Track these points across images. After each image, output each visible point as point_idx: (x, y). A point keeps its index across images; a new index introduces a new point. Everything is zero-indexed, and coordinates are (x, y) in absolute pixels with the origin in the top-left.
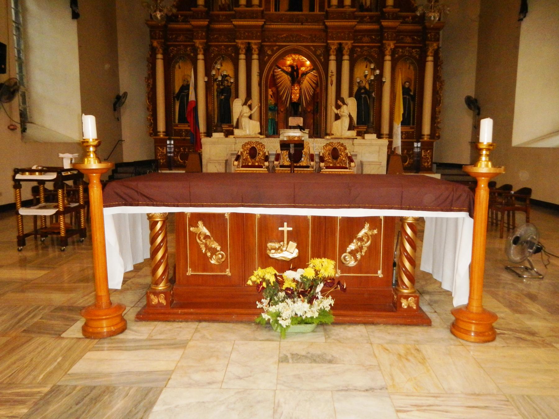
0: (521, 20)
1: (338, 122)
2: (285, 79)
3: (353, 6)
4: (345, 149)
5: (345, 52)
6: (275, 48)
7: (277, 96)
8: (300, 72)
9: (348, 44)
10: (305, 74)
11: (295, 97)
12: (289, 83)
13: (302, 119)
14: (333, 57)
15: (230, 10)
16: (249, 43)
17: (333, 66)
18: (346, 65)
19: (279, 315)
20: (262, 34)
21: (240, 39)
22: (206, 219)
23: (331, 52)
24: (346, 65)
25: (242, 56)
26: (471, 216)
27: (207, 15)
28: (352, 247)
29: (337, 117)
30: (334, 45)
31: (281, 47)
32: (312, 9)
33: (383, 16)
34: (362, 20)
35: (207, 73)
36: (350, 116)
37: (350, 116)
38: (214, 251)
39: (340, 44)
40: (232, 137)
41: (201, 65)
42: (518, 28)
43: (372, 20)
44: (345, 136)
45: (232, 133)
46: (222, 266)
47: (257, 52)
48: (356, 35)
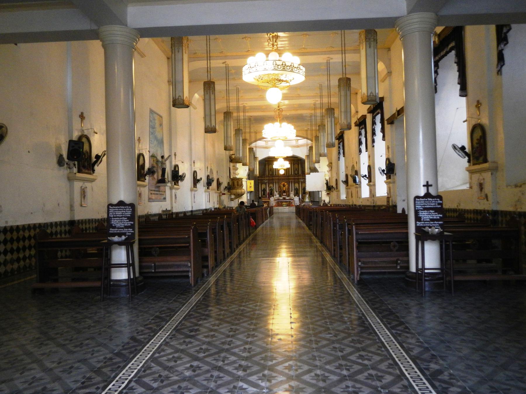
2: (282, 186)
9: (293, 181)
20: (278, 179)
27: (269, 177)
33: (299, 176)
35: (268, 186)
41: (267, 185)
48: (294, 179)
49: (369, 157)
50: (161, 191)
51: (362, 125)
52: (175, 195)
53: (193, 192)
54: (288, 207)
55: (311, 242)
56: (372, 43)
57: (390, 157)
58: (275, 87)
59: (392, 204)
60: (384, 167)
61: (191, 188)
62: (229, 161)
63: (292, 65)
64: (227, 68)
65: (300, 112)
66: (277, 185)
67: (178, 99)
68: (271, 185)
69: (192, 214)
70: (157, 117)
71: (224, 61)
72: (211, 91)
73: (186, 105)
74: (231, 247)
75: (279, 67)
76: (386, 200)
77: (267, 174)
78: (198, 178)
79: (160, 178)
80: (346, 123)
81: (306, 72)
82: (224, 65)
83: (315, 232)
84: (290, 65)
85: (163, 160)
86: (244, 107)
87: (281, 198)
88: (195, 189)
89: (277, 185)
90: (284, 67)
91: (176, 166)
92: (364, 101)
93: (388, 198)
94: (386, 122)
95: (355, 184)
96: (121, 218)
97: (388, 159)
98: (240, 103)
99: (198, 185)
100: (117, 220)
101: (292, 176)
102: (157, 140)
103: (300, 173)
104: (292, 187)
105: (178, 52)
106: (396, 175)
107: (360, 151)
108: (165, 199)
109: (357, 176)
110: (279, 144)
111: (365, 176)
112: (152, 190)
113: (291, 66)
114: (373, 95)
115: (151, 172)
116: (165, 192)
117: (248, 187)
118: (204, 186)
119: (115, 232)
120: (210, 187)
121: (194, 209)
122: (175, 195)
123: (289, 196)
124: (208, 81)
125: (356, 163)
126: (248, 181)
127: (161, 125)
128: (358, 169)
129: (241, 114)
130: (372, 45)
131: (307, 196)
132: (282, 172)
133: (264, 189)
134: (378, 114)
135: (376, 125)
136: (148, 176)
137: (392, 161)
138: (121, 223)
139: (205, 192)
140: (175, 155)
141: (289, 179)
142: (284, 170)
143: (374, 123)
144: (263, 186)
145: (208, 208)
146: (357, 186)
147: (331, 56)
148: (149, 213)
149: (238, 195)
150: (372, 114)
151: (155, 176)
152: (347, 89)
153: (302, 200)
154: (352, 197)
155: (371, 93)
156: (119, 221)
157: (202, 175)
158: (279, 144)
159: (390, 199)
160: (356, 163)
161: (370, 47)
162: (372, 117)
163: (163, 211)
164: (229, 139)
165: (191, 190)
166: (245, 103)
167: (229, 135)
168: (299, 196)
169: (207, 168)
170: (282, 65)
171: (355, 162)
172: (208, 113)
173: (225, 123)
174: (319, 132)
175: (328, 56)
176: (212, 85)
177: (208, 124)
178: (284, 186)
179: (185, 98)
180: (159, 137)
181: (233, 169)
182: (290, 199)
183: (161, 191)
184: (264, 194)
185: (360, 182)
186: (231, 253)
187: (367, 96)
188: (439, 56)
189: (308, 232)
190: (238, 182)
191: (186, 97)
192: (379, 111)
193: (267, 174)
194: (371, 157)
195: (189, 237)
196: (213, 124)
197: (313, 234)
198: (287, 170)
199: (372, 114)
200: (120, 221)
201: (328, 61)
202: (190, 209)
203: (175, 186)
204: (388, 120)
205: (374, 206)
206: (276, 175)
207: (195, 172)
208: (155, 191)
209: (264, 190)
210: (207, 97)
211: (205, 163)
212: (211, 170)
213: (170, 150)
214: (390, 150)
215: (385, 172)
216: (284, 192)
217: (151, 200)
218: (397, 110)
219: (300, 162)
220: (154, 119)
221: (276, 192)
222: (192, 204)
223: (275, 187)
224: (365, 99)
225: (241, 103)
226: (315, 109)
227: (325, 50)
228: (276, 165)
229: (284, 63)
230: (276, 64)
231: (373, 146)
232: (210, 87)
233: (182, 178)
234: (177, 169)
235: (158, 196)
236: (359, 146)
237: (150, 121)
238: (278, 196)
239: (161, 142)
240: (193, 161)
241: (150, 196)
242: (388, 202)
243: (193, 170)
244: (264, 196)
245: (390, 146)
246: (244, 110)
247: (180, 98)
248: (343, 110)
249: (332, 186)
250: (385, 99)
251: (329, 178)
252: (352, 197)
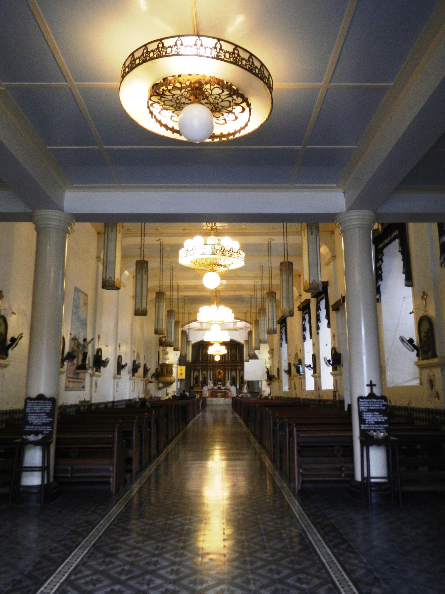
2: (217, 374)
3: (230, 361)
7: (215, 376)
9: (230, 368)
10: (221, 373)
11: (220, 378)
17: (227, 372)
20: (213, 366)
27: (202, 363)
30: (227, 368)
33: (236, 363)
41: (200, 372)
43: (235, 363)
48: (231, 366)
49: (314, 345)
50: (80, 379)
51: (306, 310)
52: (96, 383)
53: (116, 380)
54: (223, 399)
55: (249, 442)
56: (314, 230)
57: (336, 346)
58: (213, 271)
59: (339, 399)
60: (329, 357)
61: (114, 375)
62: (158, 345)
63: (232, 250)
64: (162, 246)
65: (238, 293)
66: (211, 372)
67: (109, 280)
68: (205, 373)
69: (113, 406)
70: (82, 296)
71: (158, 238)
72: (144, 270)
73: (116, 287)
74: (157, 447)
75: (218, 251)
76: (332, 394)
77: (201, 359)
78: (123, 363)
79: (80, 363)
80: (288, 309)
81: (246, 256)
82: (159, 242)
83: (253, 430)
84: (229, 250)
85: (86, 344)
86: (178, 286)
87: (216, 388)
88: (118, 376)
89: (211, 372)
90: (223, 252)
91: (99, 350)
92: (306, 288)
93: (335, 392)
94: (331, 309)
95: (298, 374)
96: (39, 414)
97: (333, 349)
98: (174, 282)
99: (123, 372)
100: (35, 416)
101: (229, 363)
102: (80, 321)
103: (238, 359)
104: (229, 375)
105: (112, 231)
106: (342, 366)
107: (304, 338)
108: (84, 387)
109: (300, 366)
110: (216, 328)
111: (310, 366)
112: (70, 378)
113: (230, 251)
114: (315, 283)
115: (71, 356)
116: (84, 379)
117: (179, 374)
118: (129, 373)
119: (31, 429)
120: (136, 374)
121: (116, 399)
122: (96, 383)
123: (224, 385)
124: (141, 260)
125: (300, 351)
126: (179, 367)
127: (86, 304)
128: (301, 358)
129: (175, 293)
130: (314, 233)
131: (246, 386)
132: (217, 358)
134: (322, 299)
135: (321, 310)
136: (67, 361)
137: (338, 351)
138: (38, 419)
139: (130, 379)
140: (99, 337)
141: (225, 366)
142: (220, 356)
143: (318, 308)
144: (196, 373)
145: (132, 398)
146: (301, 376)
147: (273, 237)
148: (65, 404)
149: (167, 383)
150: (316, 299)
151: (75, 361)
152: (289, 274)
153: (239, 391)
154: (295, 389)
155: (314, 281)
156: (36, 417)
157: (127, 360)
158: (216, 328)
159: (337, 393)
160: (300, 351)
161: (312, 234)
162: (316, 301)
163: (81, 402)
164: (160, 322)
165: (114, 378)
166: (179, 281)
167: (161, 317)
168: (236, 386)
169: (134, 352)
170: (221, 249)
171: (299, 350)
172: (139, 294)
173: (157, 304)
174: (260, 316)
175: (269, 237)
176: (145, 265)
177: (139, 306)
178: (219, 373)
179: (116, 280)
180: (83, 316)
181: (163, 354)
182: (226, 389)
183: (80, 379)
184: (196, 383)
185: (304, 372)
186: (159, 453)
187: (310, 284)
188: (383, 244)
189: (245, 429)
190: (167, 369)
191: (118, 279)
192: (323, 296)
193: (201, 359)
194: (316, 345)
195: (113, 437)
196: (144, 306)
197: (251, 432)
198: (223, 356)
199: (316, 299)
200: (38, 417)
201: (269, 242)
202: (111, 399)
203: (97, 373)
204: (332, 306)
205: (320, 401)
207: (120, 357)
208: (73, 378)
209: (197, 378)
210: (139, 276)
211: (132, 346)
212: (138, 354)
213: (94, 333)
214: (336, 338)
215: (331, 363)
216: (220, 380)
217: (68, 389)
218: (342, 296)
219: (238, 347)
220: (79, 298)
221: (211, 380)
222: (114, 393)
223: (210, 375)
224: (308, 287)
225: (175, 283)
226: (255, 290)
227: (267, 231)
228: (211, 351)
229: (223, 248)
230: (215, 249)
231: (318, 334)
232: (143, 267)
233: (105, 363)
234: (100, 354)
235: (75, 384)
236: (303, 333)
237: (75, 300)
238: (212, 385)
239: (84, 324)
240: (118, 345)
241: (67, 385)
242: (335, 396)
243: (118, 354)
244: (196, 385)
245: (336, 335)
246: (178, 289)
247: (110, 279)
248: (285, 295)
249: (274, 376)
250: (329, 284)
251: (271, 366)
252: (295, 389)
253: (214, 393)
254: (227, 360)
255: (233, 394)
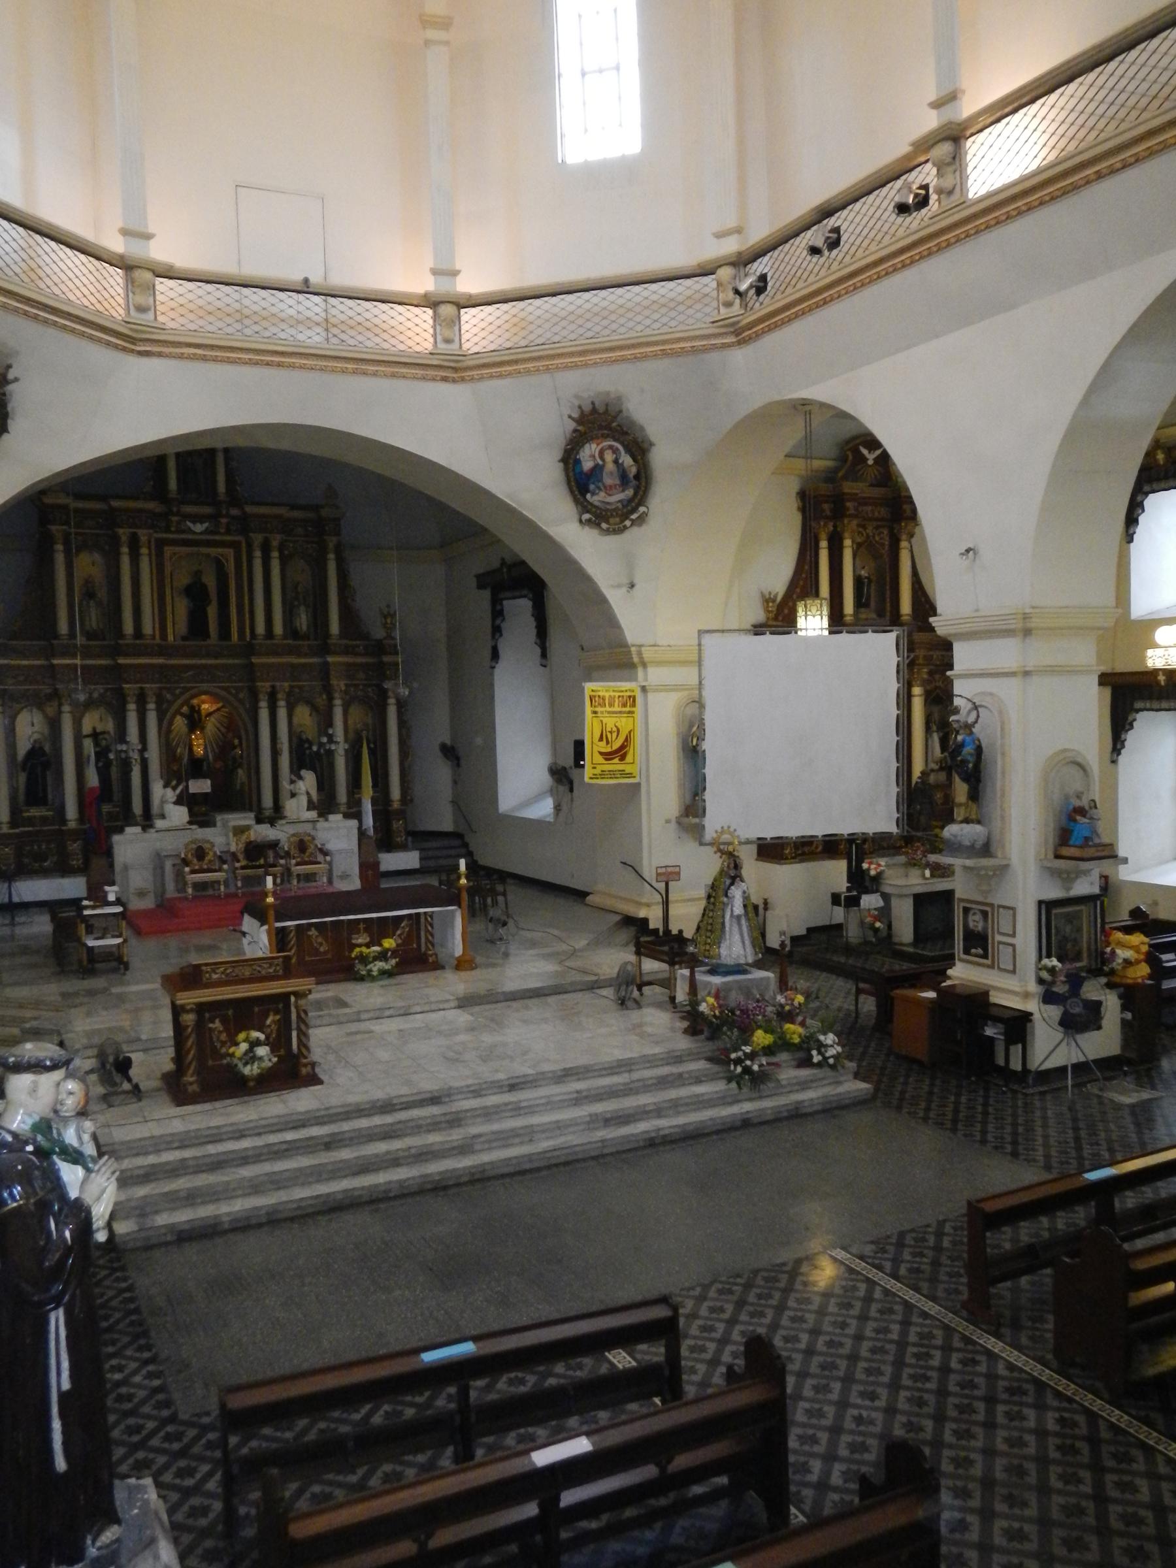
0: (493, 668)
1: (294, 801)
3: (285, 637)
4: (314, 839)
5: (280, 696)
6: (177, 692)
8: (203, 713)
12: (185, 729)
13: (209, 782)
14: (263, 704)
15: (104, 639)
16: (142, 688)
17: (264, 714)
18: (282, 713)
19: (371, 970)
21: (127, 683)
22: (320, 927)
23: (261, 696)
24: (282, 713)
25: (132, 706)
26: (460, 906)
28: (399, 932)
29: (293, 795)
30: (264, 686)
31: (187, 689)
32: (225, 634)
34: (297, 652)
36: (308, 793)
37: (308, 793)
38: (321, 944)
39: (273, 687)
40: (152, 830)
42: (492, 674)
44: (303, 819)
45: (151, 826)
46: (325, 953)
47: (154, 699)
103: (335, 628)
133: (35, 752)
168: (354, 812)
206: (138, 633)
244: (35, 812)
253: (313, 932)
254: (260, 629)
255: (345, 876)
